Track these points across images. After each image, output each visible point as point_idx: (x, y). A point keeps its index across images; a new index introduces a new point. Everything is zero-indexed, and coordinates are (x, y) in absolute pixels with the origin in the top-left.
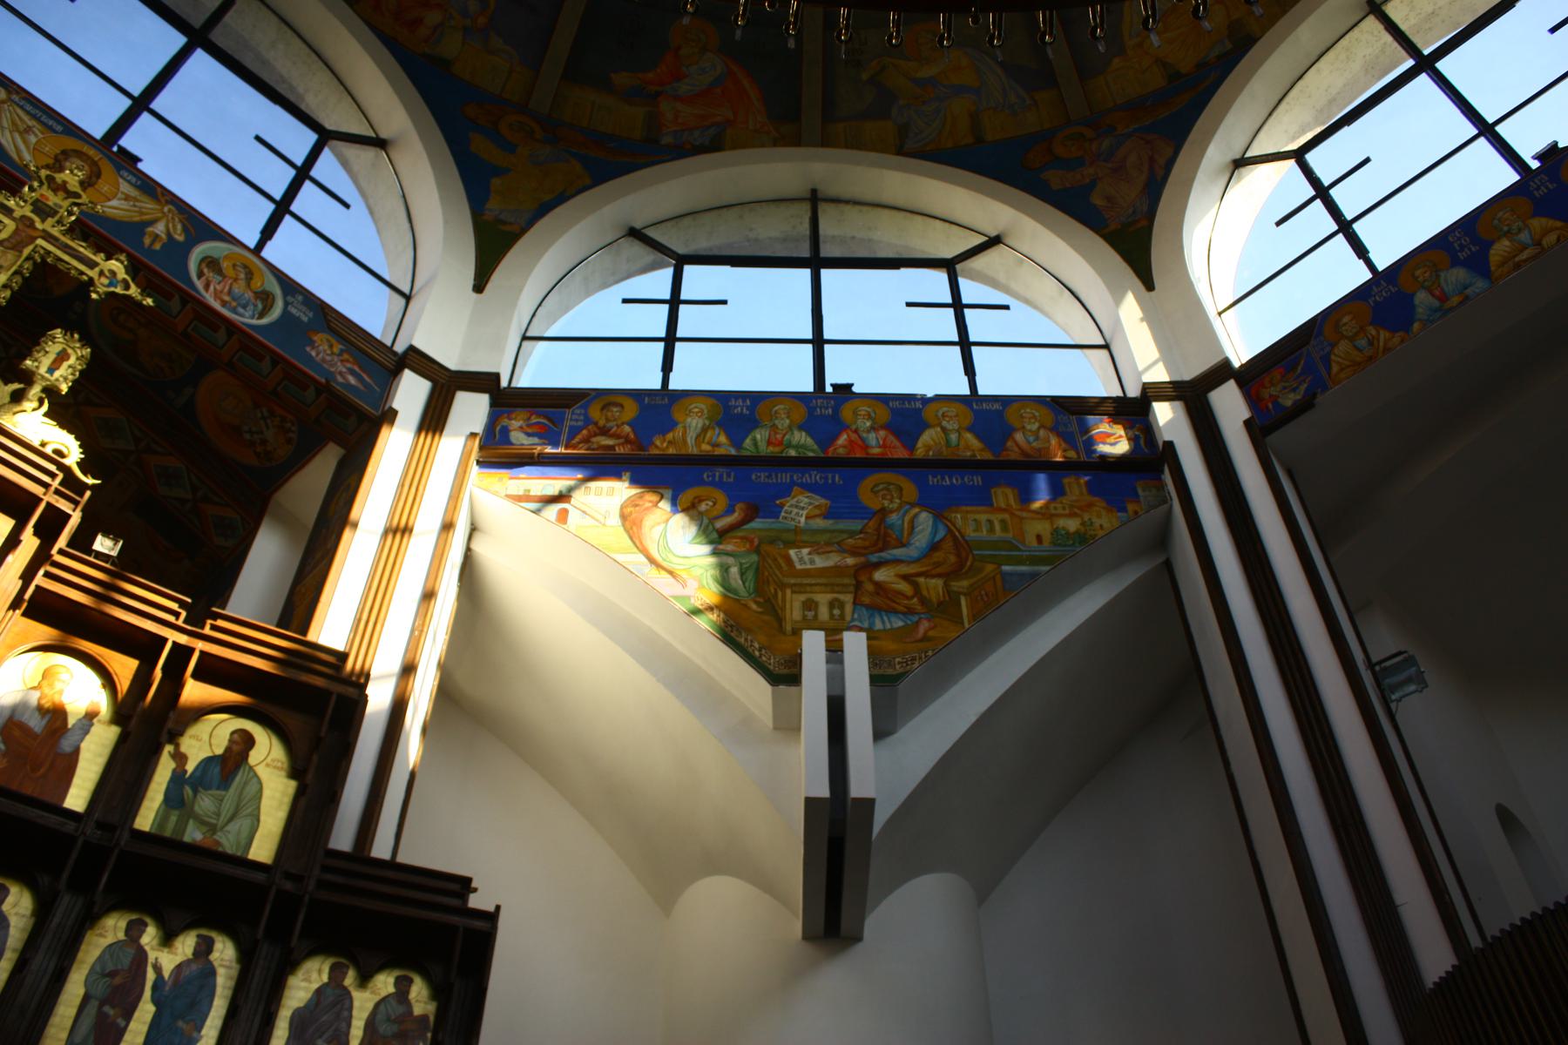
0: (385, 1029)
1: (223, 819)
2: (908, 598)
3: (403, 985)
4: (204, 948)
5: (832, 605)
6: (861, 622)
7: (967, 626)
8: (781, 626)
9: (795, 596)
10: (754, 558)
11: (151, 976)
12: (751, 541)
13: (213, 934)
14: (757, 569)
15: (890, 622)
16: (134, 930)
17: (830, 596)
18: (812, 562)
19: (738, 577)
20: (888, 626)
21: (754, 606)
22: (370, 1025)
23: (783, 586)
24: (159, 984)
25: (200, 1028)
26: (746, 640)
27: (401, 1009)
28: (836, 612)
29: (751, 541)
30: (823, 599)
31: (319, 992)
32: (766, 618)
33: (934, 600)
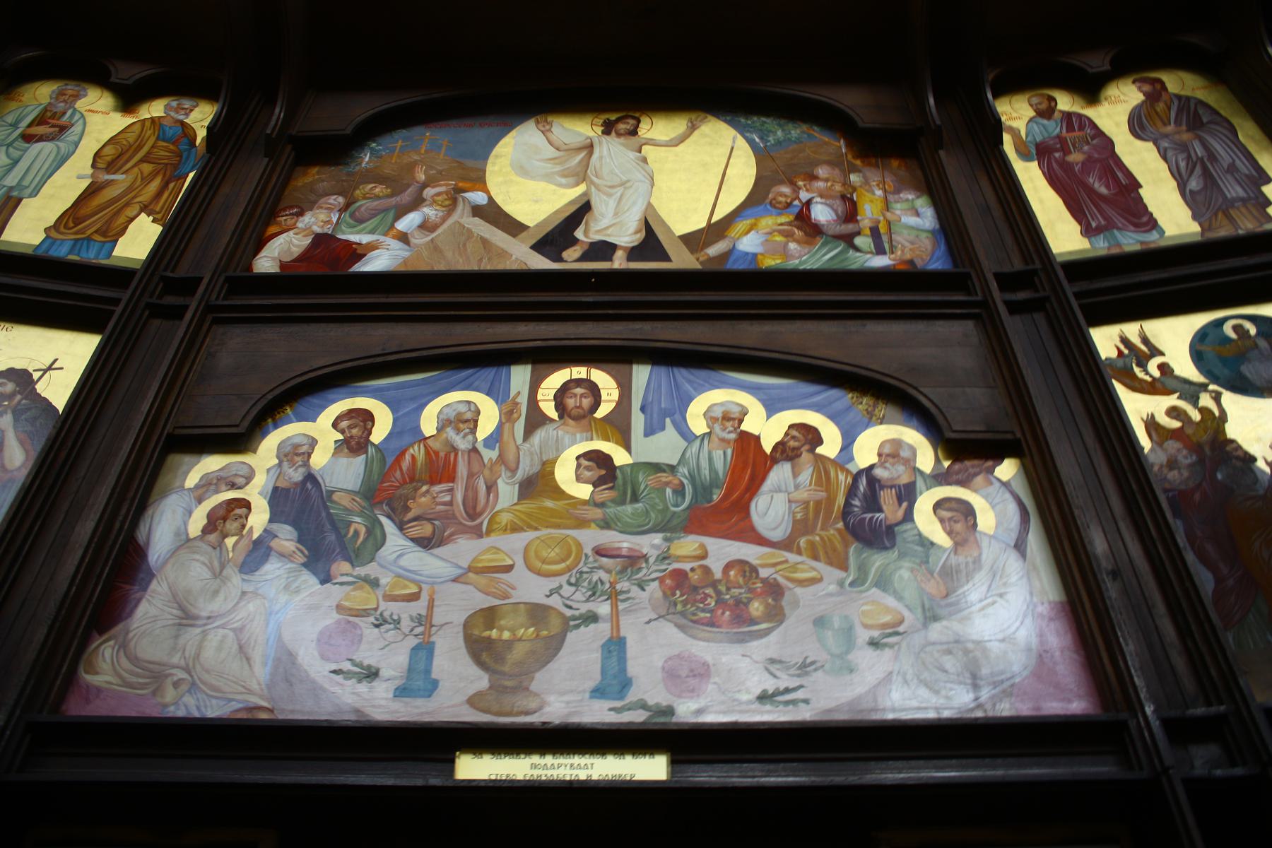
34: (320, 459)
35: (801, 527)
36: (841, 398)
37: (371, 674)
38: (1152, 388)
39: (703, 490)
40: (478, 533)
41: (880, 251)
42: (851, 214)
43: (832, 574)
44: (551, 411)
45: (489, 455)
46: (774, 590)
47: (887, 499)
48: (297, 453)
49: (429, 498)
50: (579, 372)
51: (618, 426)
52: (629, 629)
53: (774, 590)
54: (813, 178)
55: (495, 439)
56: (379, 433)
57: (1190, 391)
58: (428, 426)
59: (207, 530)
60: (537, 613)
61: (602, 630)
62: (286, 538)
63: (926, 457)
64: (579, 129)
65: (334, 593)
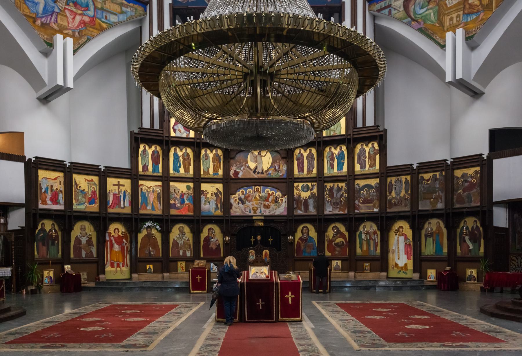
0: (372, 153)
1: (336, 129)
2: (478, 6)
3: (373, 145)
4: (341, 148)
5: (457, 17)
6: (464, 20)
7: (494, 11)
8: (444, 29)
9: (448, 17)
10: (437, 7)
11: (335, 155)
12: (436, 2)
13: (341, 146)
14: (438, 11)
15: (472, 17)
16: (330, 149)
17: (456, 14)
18: (452, 3)
19: (433, 16)
20: (472, 19)
21: (437, 25)
22: (369, 153)
23: (444, 15)
24: (336, 157)
25: (344, 161)
26: (435, 37)
27: (374, 149)
28: (458, 19)
29: (436, 2)
30: (454, 16)
31: (360, 150)
32: (440, 27)
33: (486, 4)
34: (241, 195)
35: (272, 201)
36: (276, 189)
37: (247, 211)
38: (297, 190)
39: (266, 198)
40: (252, 201)
41: (281, 173)
42: (279, 168)
43: (273, 204)
44: (256, 191)
45: (252, 195)
46: (270, 206)
47: (277, 199)
48: (239, 195)
49: (249, 199)
50: (257, 187)
51: (260, 192)
52: (261, 208)
53: (270, 206)
54: (277, 162)
55: (252, 193)
56: (244, 193)
57: (300, 190)
58: (248, 193)
59: (235, 201)
60: (256, 207)
61: (260, 208)
62: (240, 202)
63: (281, 195)
64: (256, 153)
65: (244, 206)
